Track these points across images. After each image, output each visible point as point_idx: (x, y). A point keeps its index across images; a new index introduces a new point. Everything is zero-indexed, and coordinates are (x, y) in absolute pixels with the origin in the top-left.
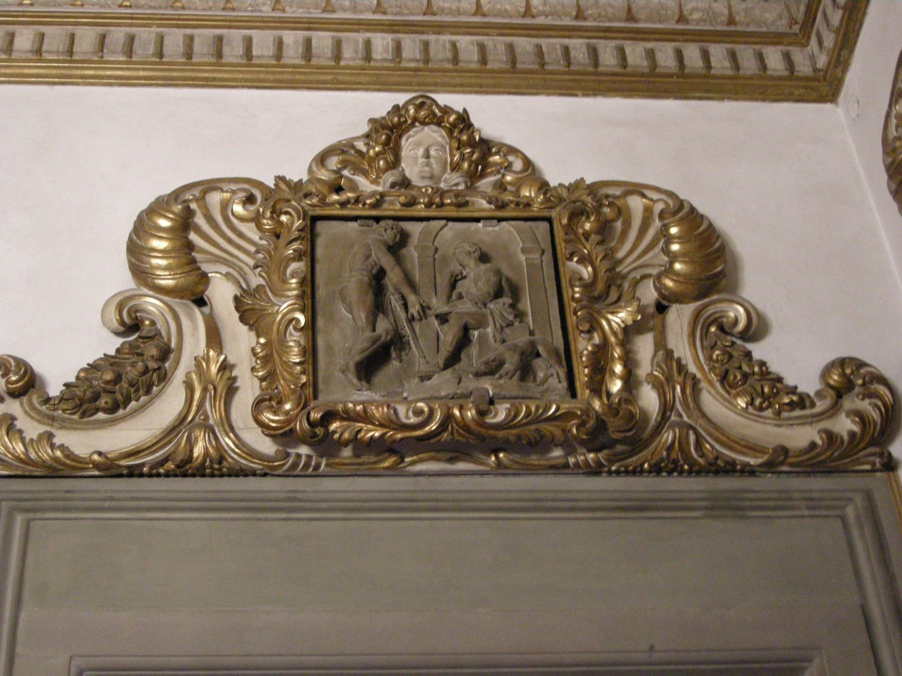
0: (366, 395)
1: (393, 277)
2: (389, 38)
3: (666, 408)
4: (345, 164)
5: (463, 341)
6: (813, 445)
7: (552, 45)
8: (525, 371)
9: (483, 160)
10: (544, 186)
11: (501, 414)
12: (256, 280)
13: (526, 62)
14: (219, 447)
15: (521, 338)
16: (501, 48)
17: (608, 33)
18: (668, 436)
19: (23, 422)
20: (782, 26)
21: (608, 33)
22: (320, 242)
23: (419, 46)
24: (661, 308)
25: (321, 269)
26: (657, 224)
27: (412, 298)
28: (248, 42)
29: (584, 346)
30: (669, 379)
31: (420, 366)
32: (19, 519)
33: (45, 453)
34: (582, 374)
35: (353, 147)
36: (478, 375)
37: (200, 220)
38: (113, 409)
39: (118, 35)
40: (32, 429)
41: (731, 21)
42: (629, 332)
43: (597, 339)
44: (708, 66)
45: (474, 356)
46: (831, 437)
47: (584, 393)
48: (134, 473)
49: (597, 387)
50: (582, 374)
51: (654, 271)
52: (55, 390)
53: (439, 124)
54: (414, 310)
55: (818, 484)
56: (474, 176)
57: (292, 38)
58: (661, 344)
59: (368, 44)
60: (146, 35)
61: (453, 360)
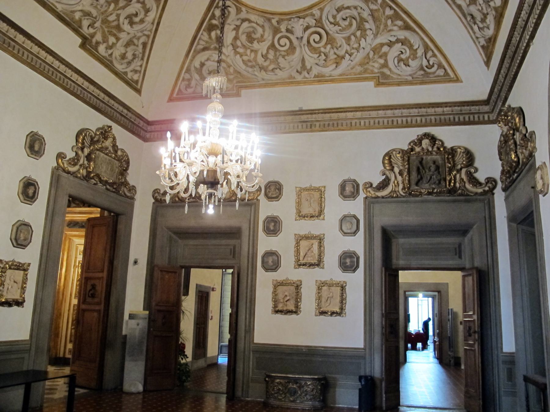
0: (417, 188)
1: (421, 168)
3: (460, 187)
4: (414, 144)
5: (431, 178)
6: (481, 192)
7: (447, 117)
8: (440, 183)
9: (435, 141)
10: (445, 148)
11: (435, 191)
12: (401, 168)
13: (443, 121)
14: (397, 195)
15: (439, 177)
17: (457, 114)
18: (460, 191)
19: (371, 192)
20: (488, 110)
21: (457, 114)
22: (410, 161)
24: (461, 169)
25: (411, 165)
26: (462, 154)
27: (424, 171)
28: (397, 120)
29: (448, 178)
30: (461, 182)
31: (425, 182)
32: (372, 205)
33: (373, 196)
34: (448, 184)
35: (414, 141)
36: (433, 184)
37: (392, 157)
38: (383, 189)
39: (377, 121)
40: (372, 192)
41: (479, 110)
42: (456, 175)
43: (450, 177)
44: (474, 119)
45: (432, 181)
46: (484, 191)
47: (448, 186)
48: (386, 198)
49: (450, 185)
50: (448, 184)
51: (461, 163)
52: (374, 186)
54: (424, 172)
55: (482, 197)
56: (433, 147)
57: (404, 119)
58: (460, 176)
60: (381, 120)
61: (430, 180)
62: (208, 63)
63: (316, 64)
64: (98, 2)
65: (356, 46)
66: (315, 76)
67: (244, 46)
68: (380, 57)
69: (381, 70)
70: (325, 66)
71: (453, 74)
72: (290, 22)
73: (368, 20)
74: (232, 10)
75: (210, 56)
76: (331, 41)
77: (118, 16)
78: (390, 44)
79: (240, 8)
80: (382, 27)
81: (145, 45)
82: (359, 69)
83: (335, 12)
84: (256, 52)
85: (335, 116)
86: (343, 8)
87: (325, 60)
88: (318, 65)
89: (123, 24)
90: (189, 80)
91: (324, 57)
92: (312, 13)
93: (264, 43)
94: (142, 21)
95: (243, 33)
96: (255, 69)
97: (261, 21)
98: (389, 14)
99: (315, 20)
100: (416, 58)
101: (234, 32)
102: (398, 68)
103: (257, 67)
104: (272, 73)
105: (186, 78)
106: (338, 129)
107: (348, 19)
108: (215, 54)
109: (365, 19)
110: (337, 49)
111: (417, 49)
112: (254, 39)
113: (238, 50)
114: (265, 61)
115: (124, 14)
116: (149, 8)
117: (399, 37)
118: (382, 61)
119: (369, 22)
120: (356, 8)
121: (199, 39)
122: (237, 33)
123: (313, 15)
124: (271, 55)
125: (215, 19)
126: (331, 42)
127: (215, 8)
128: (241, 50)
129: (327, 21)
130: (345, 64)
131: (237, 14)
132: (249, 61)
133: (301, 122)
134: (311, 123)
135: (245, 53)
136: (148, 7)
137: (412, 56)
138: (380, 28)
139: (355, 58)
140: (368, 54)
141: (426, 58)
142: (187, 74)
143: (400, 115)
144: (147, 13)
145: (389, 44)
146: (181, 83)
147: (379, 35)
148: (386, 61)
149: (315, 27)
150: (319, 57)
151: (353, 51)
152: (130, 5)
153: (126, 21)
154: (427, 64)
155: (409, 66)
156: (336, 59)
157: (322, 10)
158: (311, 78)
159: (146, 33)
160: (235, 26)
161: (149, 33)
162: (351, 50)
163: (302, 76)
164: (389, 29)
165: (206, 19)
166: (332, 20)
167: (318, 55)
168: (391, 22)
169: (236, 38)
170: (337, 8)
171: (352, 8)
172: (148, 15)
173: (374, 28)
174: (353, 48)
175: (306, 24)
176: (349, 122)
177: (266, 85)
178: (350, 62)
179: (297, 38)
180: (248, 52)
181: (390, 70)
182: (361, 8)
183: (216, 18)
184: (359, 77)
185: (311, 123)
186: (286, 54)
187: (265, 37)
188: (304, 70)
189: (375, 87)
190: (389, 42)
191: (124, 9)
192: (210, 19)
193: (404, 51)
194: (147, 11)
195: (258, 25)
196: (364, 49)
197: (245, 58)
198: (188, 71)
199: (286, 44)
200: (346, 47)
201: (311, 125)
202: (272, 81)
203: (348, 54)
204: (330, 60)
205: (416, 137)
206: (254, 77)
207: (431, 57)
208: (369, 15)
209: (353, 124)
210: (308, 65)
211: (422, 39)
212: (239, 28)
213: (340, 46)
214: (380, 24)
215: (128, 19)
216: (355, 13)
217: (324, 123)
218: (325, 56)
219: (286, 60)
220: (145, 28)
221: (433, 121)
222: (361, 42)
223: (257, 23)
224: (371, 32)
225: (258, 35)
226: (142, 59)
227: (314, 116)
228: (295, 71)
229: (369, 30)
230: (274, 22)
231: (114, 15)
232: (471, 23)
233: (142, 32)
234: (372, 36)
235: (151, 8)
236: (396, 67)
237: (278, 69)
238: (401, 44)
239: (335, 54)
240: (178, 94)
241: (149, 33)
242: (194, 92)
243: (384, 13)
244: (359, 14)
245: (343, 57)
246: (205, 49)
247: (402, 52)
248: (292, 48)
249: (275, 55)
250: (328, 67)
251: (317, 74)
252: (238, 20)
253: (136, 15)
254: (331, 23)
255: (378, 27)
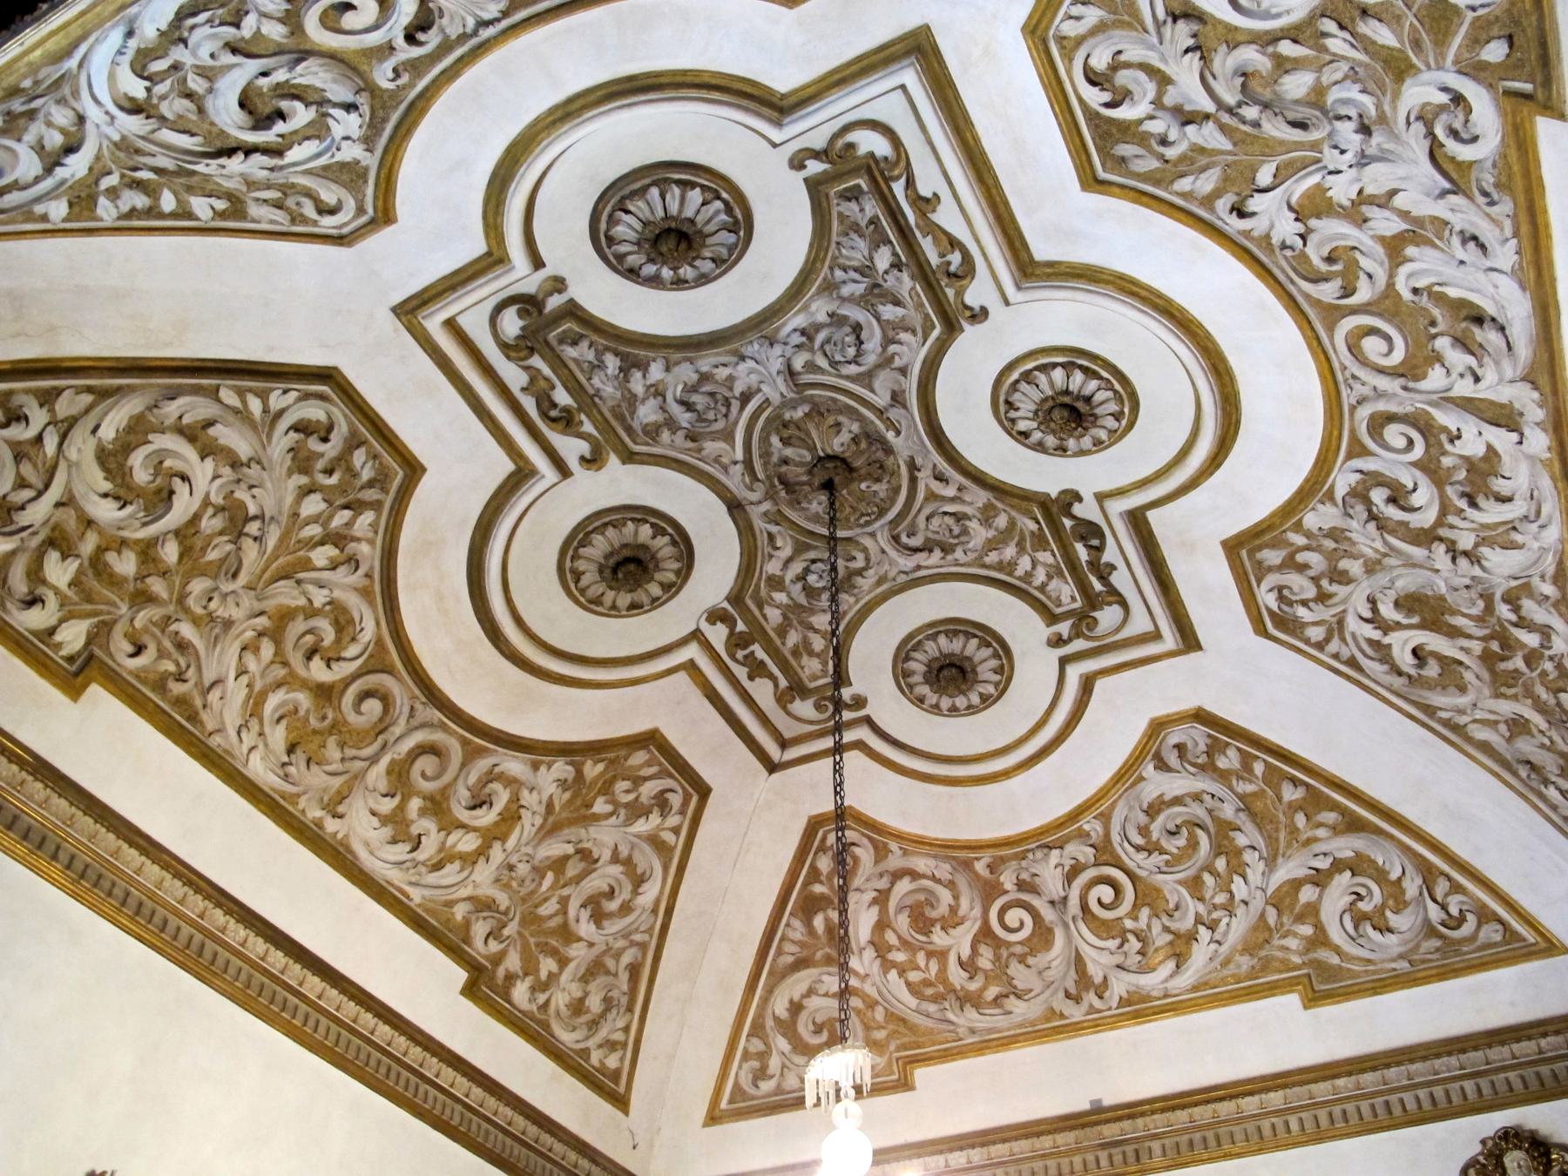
2: (1472, 1082)
13: (1549, 1082)
16: (1533, 1076)
23: (1489, 1085)
28: (1401, 1101)
35: (1478, 1162)
39: (1337, 1110)
53: (1520, 1149)
59: (1462, 1089)
62: (814, 1003)
63: (1118, 966)
64: (513, 874)
65: (1221, 899)
66: (1123, 1002)
67: (905, 944)
68: (1300, 919)
69: (1313, 955)
70: (1144, 969)
71: (1533, 933)
72: (1024, 863)
73: (1239, 822)
74: (864, 854)
75: (814, 982)
76: (1148, 896)
77: (564, 902)
78: (1320, 879)
79: (885, 845)
80: (1282, 835)
81: (634, 970)
82: (1245, 963)
83: (1143, 819)
84: (941, 955)
85: (1202, 1113)
86: (1163, 803)
87: (1141, 953)
88: (1124, 969)
89: (578, 921)
90: (763, 1056)
91: (1137, 945)
92: (1080, 828)
93: (960, 929)
94: (626, 909)
95: (900, 910)
96: (947, 1005)
97: (944, 870)
98: (1294, 797)
99: (1091, 846)
100: (1406, 904)
101: (875, 910)
102: (1360, 941)
103: (952, 997)
104: (997, 1011)
105: (752, 1049)
106: (1220, 1153)
107: (1184, 831)
108: (829, 974)
109: (1230, 823)
110: (1171, 916)
111: (1399, 879)
112: (933, 922)
113: (891, 956)
114: (971, 978)
115: (577, 896)
116: (643, 874)
117: (1339, 855)
118: (1307, 930)
119: (1243, 828)
120: (1197, 797)
121: (782, 939)
122: (884, 911)
123: (1083, 835)
124: (985, 962)
125: (821, 882)
126: (1148, 900)
127: (816, 853)
128: (900, 957)
129: (1126, 844)
130: (1200, 954)
131: (877, 862)
132: (927, 983)
133: (1104, 1146)
134: (1136, 1146)
135: (911, 961)
136: (639, 871)
137: (1391, 902)
138: (1277, 840)
139: (1226, 933)
140: (1262, 915)
141: (1435, 901)
142: (755, 1041)
143: (1405, 1082)
144: (639, 886)
145: (1315, 880)
146: (740, 1067)
147: (1280, 860)
148: (1319, 928)
149: (1094, 865)
150: (1121, 945)
151: (1215, 915)
152: (595, 870)
153: (585, 915)
154: (1443, 916)
155: (1390, 930)
156: (1171, 943)
157: (1105, 818)
158: (1110, 1009)
159: (638, 937)
160: (874, 894)
161: (646, 937)
162: (1209, 913)
163: (1084, 1006)
164: (1304, 837)
165: (794, 886)
166: (1139, 841)
167: (1118, 941)
168: (1304, 819)
169: (882, 925)
170: (1145, 806)
171: (1188, 800)
172: (641, 890)
173: (1260, 842)
174: (1215, 907)
175: (1068, 863)
176: (1251, 1126)
177: (982, 1048)
178: (1214, 946)
179: (1052, 902)
180: (921, 958)
181: (1337, 950)
182: (1213, 796)
183: (823, 878)
184: (1250, 987)
185: (1136, 1146)
186: (1027, 950)
187: (961, 913)
188: (1087, 989)
189: (1306, 1008)
190: (1314, 872)
191: (577, 883)
192: (806, 884)
193: (1363, 892)
194: (639, 881)
195: (938, 881)
196: (1246, 903)
197: (914, 976)
198: (758, 1030)
199: (1022, 924)
200: (1193, 907)
201: (1137, 1151)
202: (1000, 1032)
203: (1203, 924)
204: (1156, 950)
205: (1478, 1148)
206: (945, 1026)
207: (1446, 895)
208: (1239, 810)
209: (1267, 1132)
210: (1095, 972)
211: (1407, 849)
212: (887, 900)
213: (1177, 908)
214: (1277, 830)
215: (589, 908)
216: (1198, 811)
217: (1177, 1139)
218: (1139, 940)
219: (1029, 966)
220: (635, 926)
221: (1518, 1085)
222: (1233, 887)
223: (934, 878)
224: (1257, 854)
225: (943, 910)
226: (630, 1009)
227: (1140, 1122)
228: (1061, 994)
229: (1250, 851)
230: (980, 867)
231: (554, 900)
232: (1534, 784)
233: (626, 936)
234: (1261, 865)
235: (648, 873)
236: (1353, 939)
237: (1012, 997)
238: (1348, 874)
239: (1166, 929)
240: (730, 1102)
241: (646, 937)
242: (779, 1090)
243: (1280, 799)
244: (1210, 811)
245: (1192, 937)
246: (800, 964)
247: (1357, 894)
248: (1042, 935)
249: (997, 957)
250: (1154, 970)
251: (1125, 995)
252: (881, 875)
253: (611, 894)
254: (1138, 848)
255: (1271, 841)
